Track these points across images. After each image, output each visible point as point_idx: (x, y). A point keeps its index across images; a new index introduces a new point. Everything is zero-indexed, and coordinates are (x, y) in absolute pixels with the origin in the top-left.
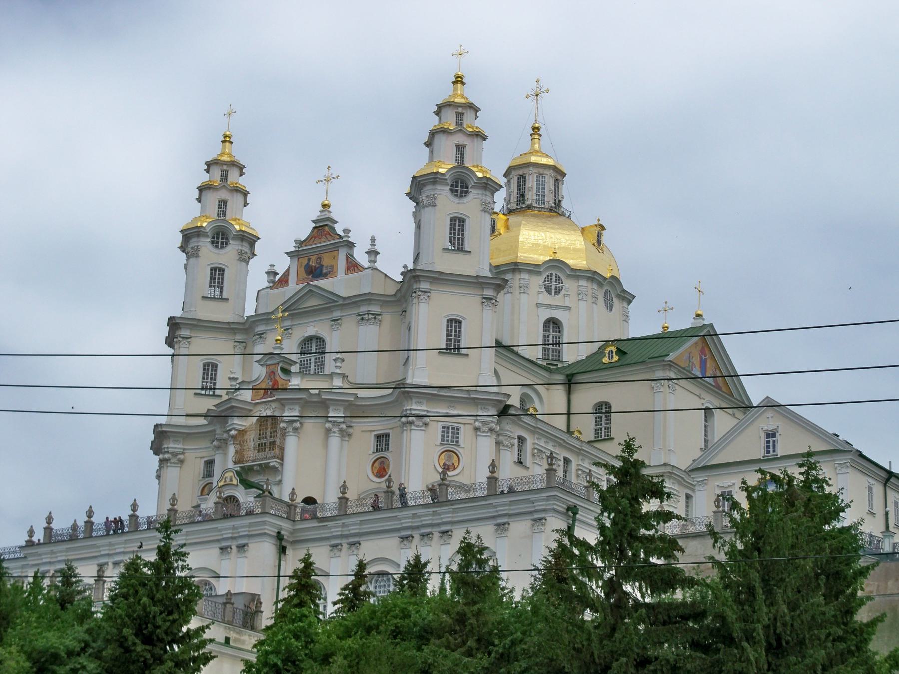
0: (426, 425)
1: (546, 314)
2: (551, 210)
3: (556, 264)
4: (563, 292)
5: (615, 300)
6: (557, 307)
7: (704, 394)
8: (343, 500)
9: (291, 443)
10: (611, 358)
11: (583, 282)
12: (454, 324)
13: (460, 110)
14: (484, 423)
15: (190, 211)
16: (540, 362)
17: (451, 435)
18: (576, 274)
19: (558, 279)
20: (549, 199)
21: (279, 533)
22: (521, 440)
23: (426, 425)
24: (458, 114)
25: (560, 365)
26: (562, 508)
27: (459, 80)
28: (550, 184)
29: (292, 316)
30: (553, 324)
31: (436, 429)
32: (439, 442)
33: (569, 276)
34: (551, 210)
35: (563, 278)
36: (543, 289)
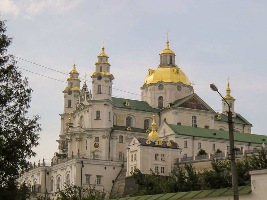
0: (91, 138)
1: (159, 96)
2: (169, 65)
3: (161, 82)
4: (164, 89)
5: (182, 88)
6: (162, 93)
7: (191, 112)
8: (39, 164)
9: (69, 144)
10: (169, 106)
11: (169, 85)
12: (98, 112)
13: (101, 58)
14: (104, 135)
15: (66, 85)
16: (157, 109)
17: (97, 139)
18: (167, 84)
19: (162, 85)
20: (168, 62)
21: (46, 170)
22: (121, 137)
23: (91, 138)
24: (101, 59)
25: (163, 108)
26: (80, 162)
27: (103, 49)
28: (168, 58)
29: (79, 111)
30: (161, 98)
31: (93, 139)
32: (94, 141)
33: (165, 84)
34: (169, 65)
35: (164, 85)
36: (158, 89)
